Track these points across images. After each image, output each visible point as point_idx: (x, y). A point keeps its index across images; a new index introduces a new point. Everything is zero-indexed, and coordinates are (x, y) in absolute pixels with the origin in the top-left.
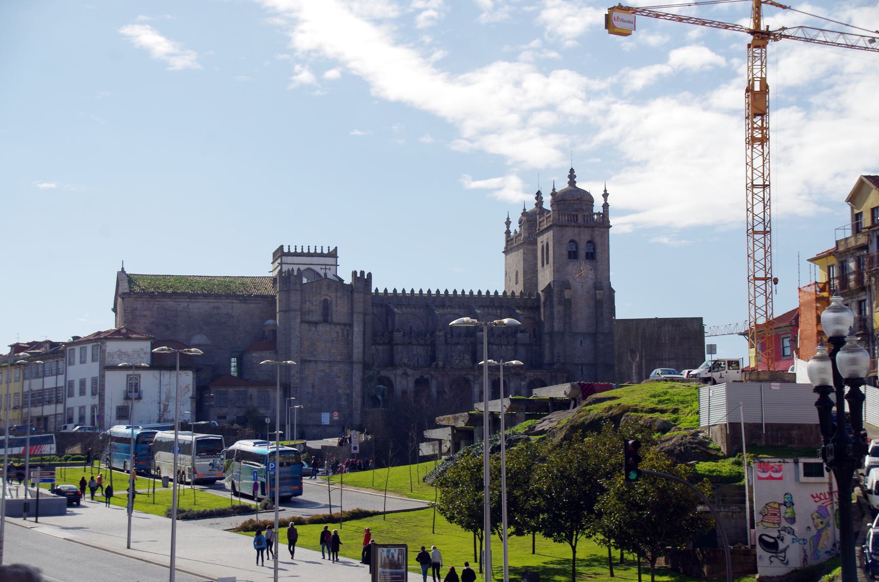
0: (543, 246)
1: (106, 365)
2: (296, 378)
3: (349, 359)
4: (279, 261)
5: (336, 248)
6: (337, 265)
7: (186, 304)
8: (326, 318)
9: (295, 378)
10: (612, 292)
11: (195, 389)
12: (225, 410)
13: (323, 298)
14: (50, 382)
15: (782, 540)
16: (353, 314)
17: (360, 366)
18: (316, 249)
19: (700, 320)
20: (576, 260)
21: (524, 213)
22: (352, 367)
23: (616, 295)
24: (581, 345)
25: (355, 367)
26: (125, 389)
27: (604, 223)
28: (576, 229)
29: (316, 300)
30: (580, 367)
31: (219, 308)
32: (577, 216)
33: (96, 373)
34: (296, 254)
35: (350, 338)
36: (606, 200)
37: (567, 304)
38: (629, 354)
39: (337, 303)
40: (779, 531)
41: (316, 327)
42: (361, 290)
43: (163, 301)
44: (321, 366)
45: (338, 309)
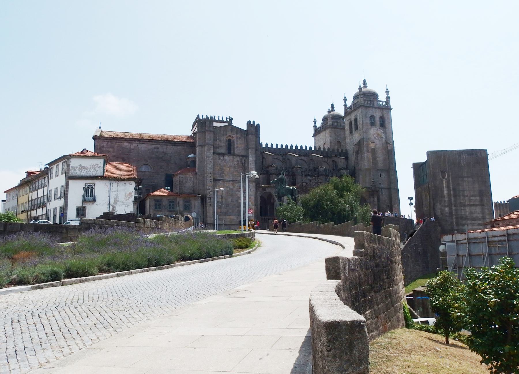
1: (70, 176)
8: (230, 151)
9: (209, 191)
13: (228, 138)
14: (41, 193)
16: (249, 149)
17: (254, 184)
18: (219, 118)
19: (485, 151)
20: (375, 127)
27: (387, 108)
29: (224, 139)
30: (381, 190)
31: (158, 148)
32: (374, 101)
33: (63, 183)
35: (246, 165)
36: (388, 95)
38: (440, 174)
39: (237, 141)
41: (223, 157)
42: (253, 133)
43: (121, 142)
45: (238, 145)
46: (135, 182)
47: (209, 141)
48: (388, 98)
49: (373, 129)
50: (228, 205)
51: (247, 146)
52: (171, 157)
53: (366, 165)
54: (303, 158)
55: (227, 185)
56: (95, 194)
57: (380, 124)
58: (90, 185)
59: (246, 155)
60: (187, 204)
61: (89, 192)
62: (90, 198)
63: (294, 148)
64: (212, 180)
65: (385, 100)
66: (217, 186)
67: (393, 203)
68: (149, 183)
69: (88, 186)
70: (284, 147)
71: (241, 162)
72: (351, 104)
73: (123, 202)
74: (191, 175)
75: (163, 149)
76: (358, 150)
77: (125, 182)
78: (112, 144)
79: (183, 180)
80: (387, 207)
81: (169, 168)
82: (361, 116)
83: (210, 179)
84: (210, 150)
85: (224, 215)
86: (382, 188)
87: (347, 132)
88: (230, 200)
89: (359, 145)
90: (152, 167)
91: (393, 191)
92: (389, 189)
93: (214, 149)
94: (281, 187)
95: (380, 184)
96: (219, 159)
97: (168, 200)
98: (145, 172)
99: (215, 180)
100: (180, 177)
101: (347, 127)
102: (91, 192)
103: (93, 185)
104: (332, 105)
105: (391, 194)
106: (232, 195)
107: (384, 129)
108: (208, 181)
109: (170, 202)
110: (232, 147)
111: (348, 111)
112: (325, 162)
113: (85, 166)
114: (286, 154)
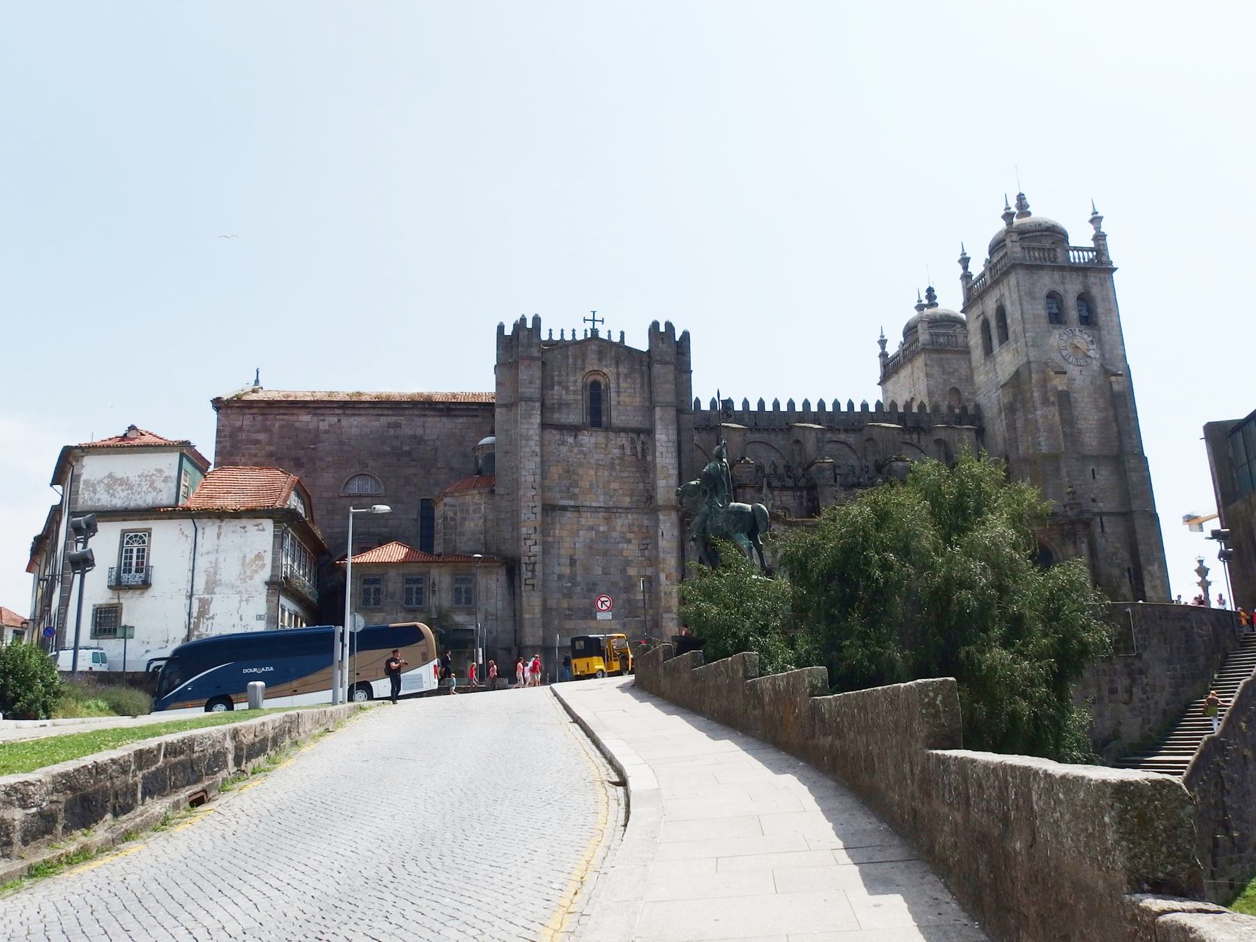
2: (531, 542)
3: (647, 504)
7: (335, 419)
9: (529, 542)
13: (591, 379)
16: (654, 408)
17: (674, 516)
22: (657, 521)
24: (1094, 478)
25: (661, 517)
26: (115, 565)
28: (1057, 275)
31: (398, 425)
35: (649, 458)
41: (576, 437)
42: (668, 359)
44: (587, 519)
45: (621, 398)
46: (274, 522)
47: (526, 390)
48: (1099, 238)
49: (1056, 332)
50: (595, 584)
51: (650, 399)
52: (436, 450)
53: (1043, 443)
54: (842, 437)
55: (590, 523)
56: (151, 564)
57: (1080, 315)
58: (136, 536)
59: (648, 426)
60: (463, 587)
61: (131, 558)
62: (134, 578)
63: (814, 408)
64: (538, 510)
65: (1092, 244)
66: (558, 526)
67: (1141, 558)
68: (372, 530)
69: (131, 538)
70: (784, 408)
72: (983, 268)
73: (233, 587)
74: (477, 497)
75: (411, 426)
76: (1015, 400)
77: (244, 522)
78: (267, 420)
79: (455, 514)
80: (1123, 574)
81: (432, 481)
82: (1015, 296)
83: (532, 504)
84: (530, 416)
85: (582, 618)
86: (1101, 514)
87: (977, 354)
88: (598, 571)
89: (1016, 382)
90: (380, 481)
91: (1139, 523)
92: (1126, 515)
93: (542, 413)
94: (710, 507)
95: (1094, 500)
97: (403, 575)
98: (360, 496)
100: (445, 505)
101: (975, 340)
102: (138, 557)
103: (142, 537)
104: (930, 291)
105: (1134, 532)
106: (605, 553)
107: (1095, 332)
108: (524, 511)
109: (409, 581)
110: (604, 406)
111: (974, 294)
112: (913, 445)
113: (125, 477)
114: (790, 429)
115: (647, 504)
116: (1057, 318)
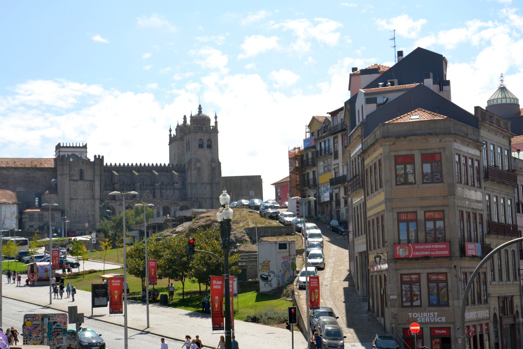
0: (187, 142)
3: (93, 197)
4: (58, 150)
5: (86, 144)
6: (87, 152)
8: (81, 178)
10: (219, 164)
11: (18, 213)
12: (33, 223)
15: (270, 276)
17: (99, 201)
19: (260, 176)
21: (178, 126)
23: (221, 164)
27: (215, 130)
30: (205, 199)
31: (29, 174)
32: (202, 128)
34: (67, 147)
35: (93, 187)
37: (199, 169)
40: (269, 273)
50: (81, 216)
54: (146, 173)
64: (69, 200)
71: (90, 185)
86: (206, 198)
95: (205, 195)
96: (74, 184)
99: (71, 199)
115: (93, 197)
116: (201, 146)
